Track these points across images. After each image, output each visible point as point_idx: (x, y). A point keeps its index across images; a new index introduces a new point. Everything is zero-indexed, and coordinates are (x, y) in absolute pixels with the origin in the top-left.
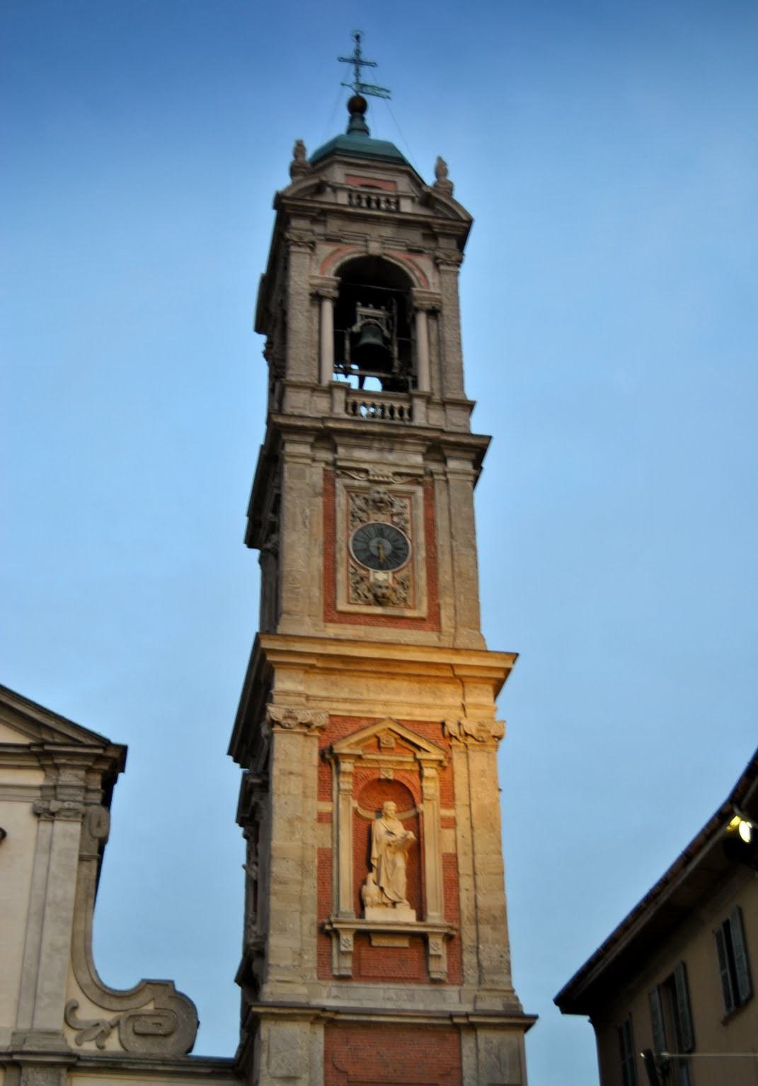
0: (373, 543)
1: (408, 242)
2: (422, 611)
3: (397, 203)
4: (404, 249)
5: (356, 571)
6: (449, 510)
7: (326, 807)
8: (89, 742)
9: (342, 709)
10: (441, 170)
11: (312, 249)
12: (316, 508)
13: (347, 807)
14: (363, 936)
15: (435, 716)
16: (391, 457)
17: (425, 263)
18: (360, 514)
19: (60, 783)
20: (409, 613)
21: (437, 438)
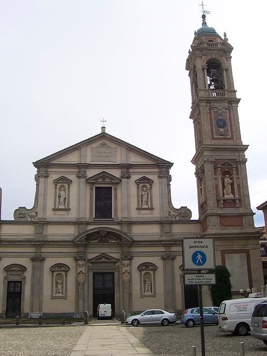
2: (230, 137)
7: (216, 177)
9: (217, 158)
10: (225, 35)
13: (219, 177)
14: (224, 201)
15: (234, 158)
16: (221, 104)
17: (224, 59)
20: (228, 137)
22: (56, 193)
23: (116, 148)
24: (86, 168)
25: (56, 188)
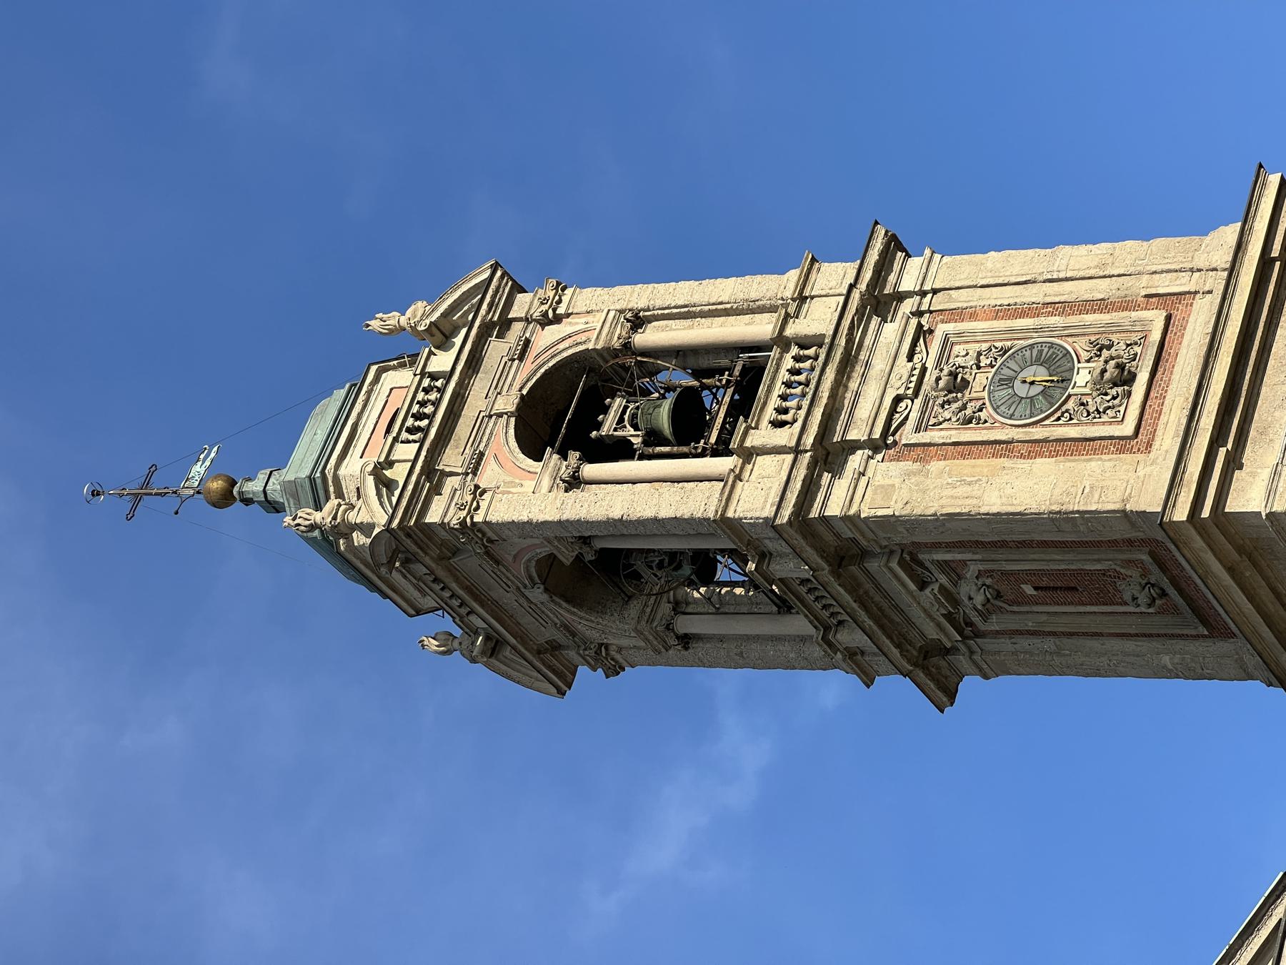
0: (1021, 390)
1: (505, 359)
2: (1156, 319)
3: (434, 377)
4: (517, 362)
5: (1067, 411)
6: (982, 287)
11: (484, 492)
12: (947, 468)
16: (879, 364)
18: (969, 412)
20: (1156, 336)
21: (862, 295)
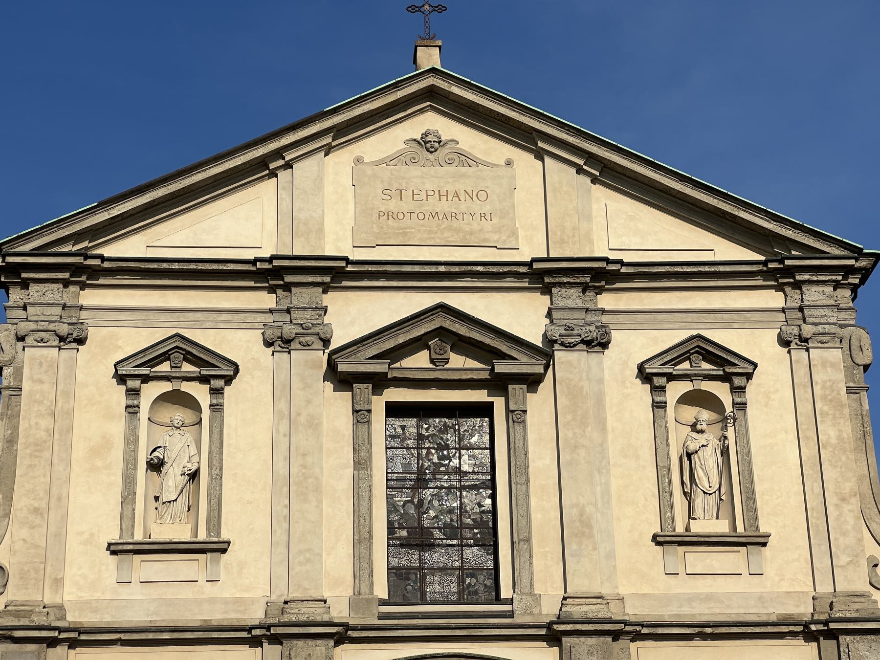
8: (836, 251)
19: (806, 303)
22: (132, 440)
23: (509, 163)
24: (326, 288)
25: (132, 410)
